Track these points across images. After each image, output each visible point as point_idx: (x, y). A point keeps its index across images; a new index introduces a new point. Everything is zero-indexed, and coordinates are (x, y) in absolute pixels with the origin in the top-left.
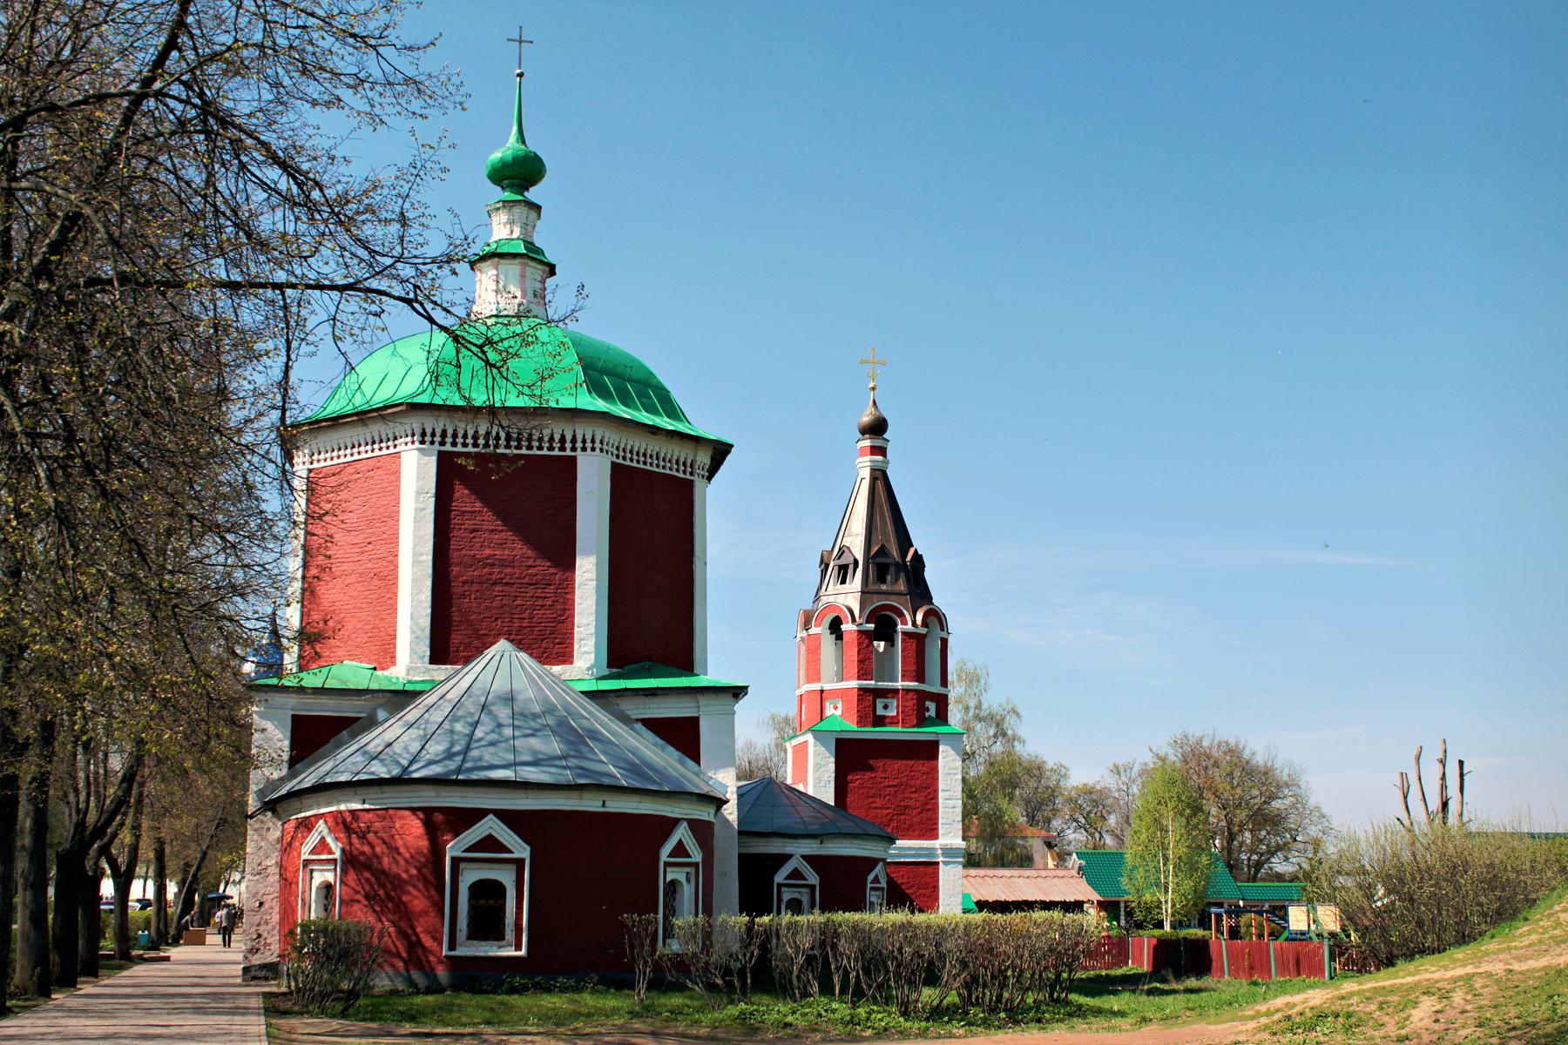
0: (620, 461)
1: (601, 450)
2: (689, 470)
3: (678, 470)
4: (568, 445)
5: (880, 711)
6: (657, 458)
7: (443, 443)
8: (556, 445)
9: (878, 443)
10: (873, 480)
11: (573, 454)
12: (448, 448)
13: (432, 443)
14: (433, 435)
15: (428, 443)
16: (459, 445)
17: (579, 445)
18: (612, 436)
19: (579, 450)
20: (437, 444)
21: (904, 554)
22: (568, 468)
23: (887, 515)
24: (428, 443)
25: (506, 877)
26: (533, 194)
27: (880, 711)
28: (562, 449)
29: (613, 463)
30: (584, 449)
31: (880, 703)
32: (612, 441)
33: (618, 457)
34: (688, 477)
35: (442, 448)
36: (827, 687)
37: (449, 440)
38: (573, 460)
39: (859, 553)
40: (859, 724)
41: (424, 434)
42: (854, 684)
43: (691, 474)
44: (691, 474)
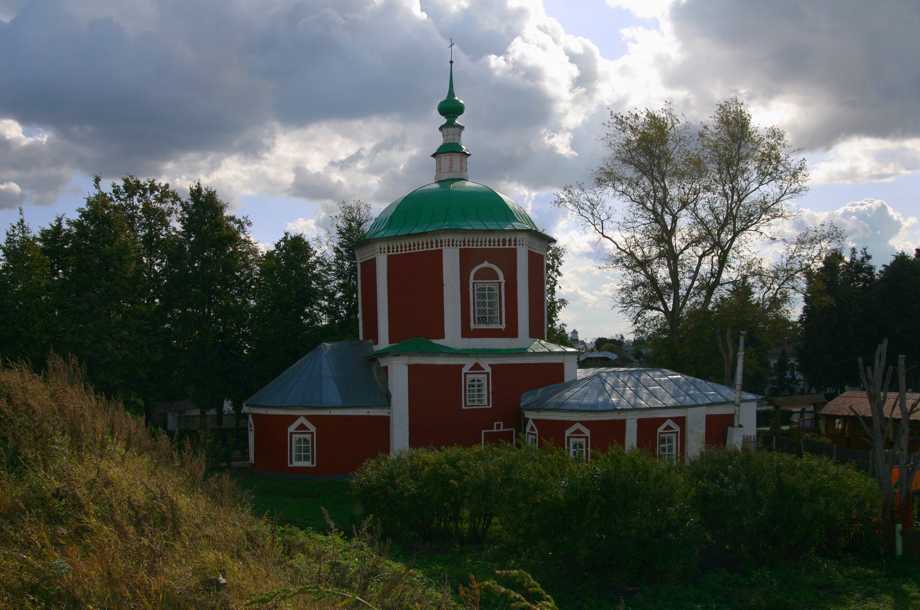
0: (467, 247)
2: (513, 243)
3: (503, 245)
4: (439, 244)
7: (389, 252)
8: (434, 245)
12: (391, 253)
14: (384, 249)
18: (458, 238)
22: (437, 256)
29: (461, 250)
30: (445, 246)
34: (513, 246)
37: (391, 250)
38: (442, 250)
41: (381, 249)
44: (515, 245)
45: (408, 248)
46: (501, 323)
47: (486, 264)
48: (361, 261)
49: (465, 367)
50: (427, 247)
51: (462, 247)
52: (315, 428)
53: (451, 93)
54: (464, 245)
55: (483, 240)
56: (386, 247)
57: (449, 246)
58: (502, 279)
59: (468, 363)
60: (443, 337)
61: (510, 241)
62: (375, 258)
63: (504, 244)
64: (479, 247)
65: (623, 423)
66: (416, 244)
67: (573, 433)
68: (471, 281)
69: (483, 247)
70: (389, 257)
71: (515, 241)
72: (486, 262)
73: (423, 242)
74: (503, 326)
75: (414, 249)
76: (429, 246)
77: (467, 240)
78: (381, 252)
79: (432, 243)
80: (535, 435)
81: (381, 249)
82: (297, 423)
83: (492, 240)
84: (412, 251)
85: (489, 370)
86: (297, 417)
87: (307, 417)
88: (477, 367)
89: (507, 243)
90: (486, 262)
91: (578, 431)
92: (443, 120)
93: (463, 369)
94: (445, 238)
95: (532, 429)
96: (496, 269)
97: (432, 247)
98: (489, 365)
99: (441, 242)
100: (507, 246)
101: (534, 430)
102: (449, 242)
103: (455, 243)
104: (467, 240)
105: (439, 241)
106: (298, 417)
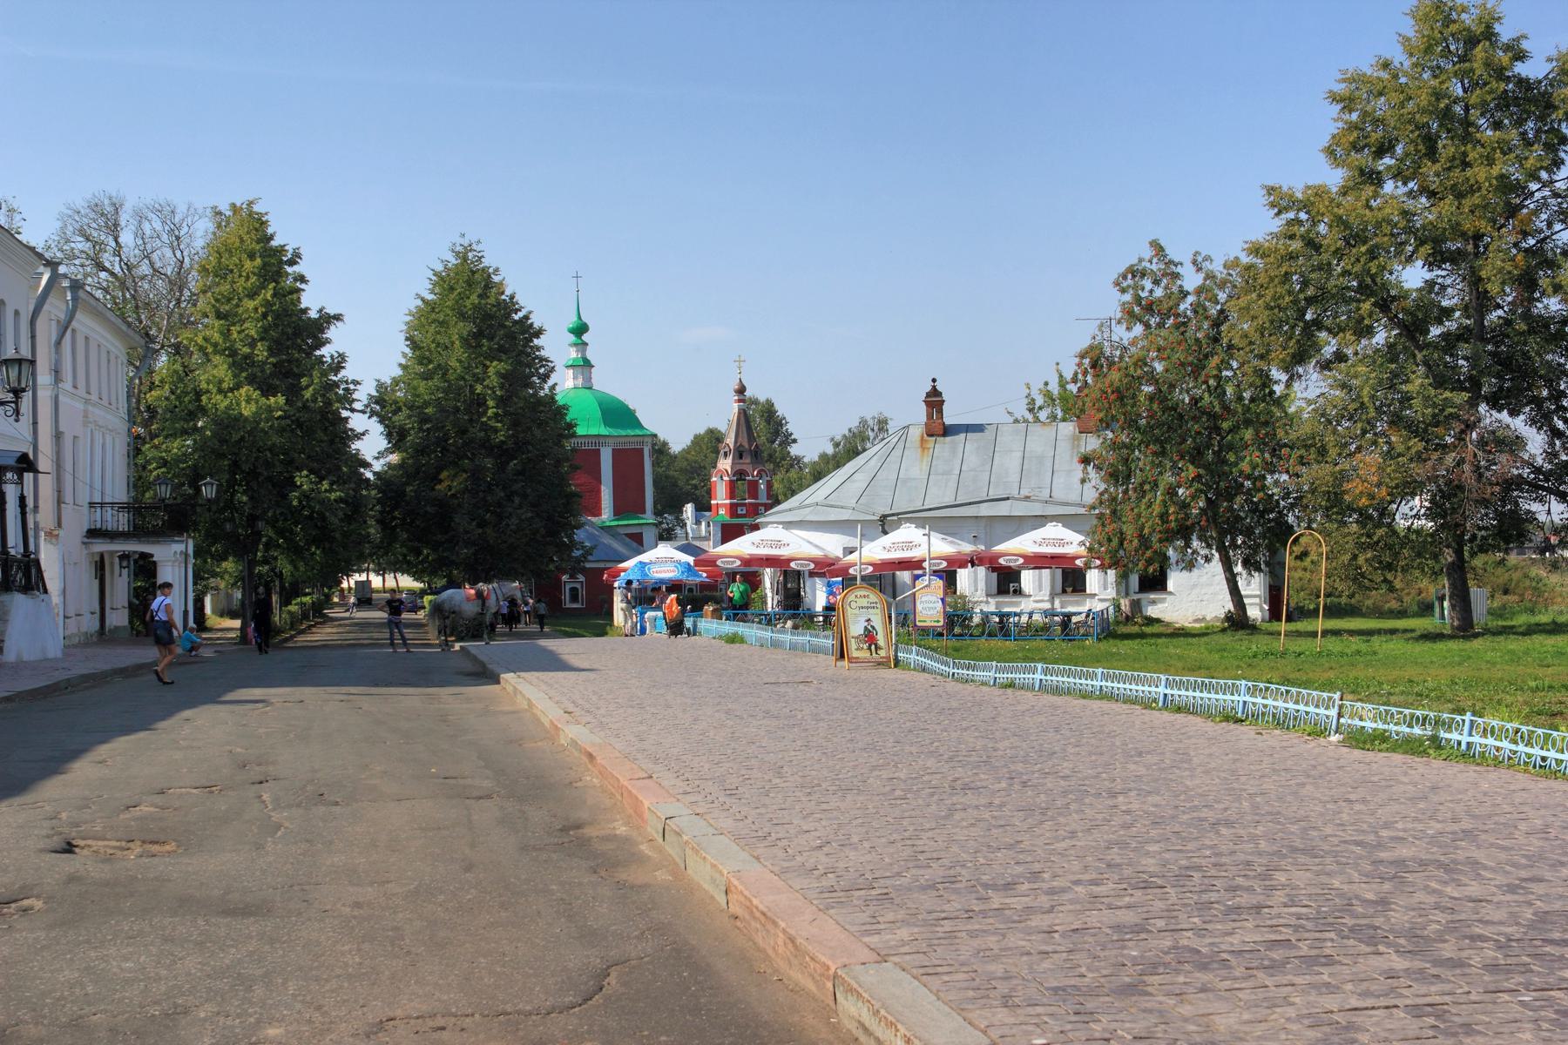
5: (739, 512)
9: (742, 397)
10: (739, 413)
18: (611, 441)
21: (750, 445)
22: (596, 454)
23: (745, 429)
25: (578, 586)
26: (585, 337)
27: (739, 512)
31: (739, 509)
36: (720, 502)
39: (732, 447)
40: (731, 517)
42: (728, 501)
53: (580, 318)
92: (572, 338)
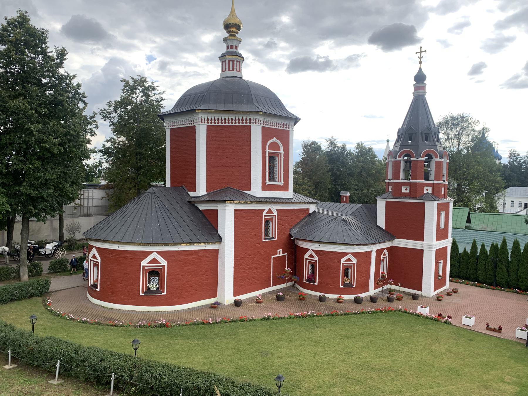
0: (265, 126)
1: (258, 123)
4: (248, 122)
6: (279, 124)
7: (208, 123)
8: (244, 122)
11: (250, 124)
12: (210, 124)
13: (204, 123)
14: (205, 120)
15: (203, 123)
16: (213, 123)
17: (252, 121)
18: (262, 119)
19: (252, 123)
20: (206, 123)
24: (203, 123)
28: (246, 123)
29: (262, 127)
30: (253, 123)
32: (262, 120)
33: (264, 124)
34: (287, 129)
35: (208, 124)
37: (210, 121)
41: (202, 120)
43: (289, 128)
45: (223, 122)
46: (281, 182)
47: (274, 140)
48: (172, 127)
49: (265, 211)
50: (239, 123)
51: (263, 126)
52: (166, 262)
54: (264, 124)
55: (274, 122)
56: (206, 119)
57: (256, 123)
58: (282, 151)
59: (266, 208)
60: (249, 189)
61: (286, 125)
62: (195, 126)
63: (283, 127)
64: (271, 127)
65: (369, 253)
66: (230, 119)
67: (345, 261)
68: (267, 151)
69: (273, 127)
70: (207, 126)
71: (289, 126)
72: (275, 138)
73: (235, 119)
74: (282, 183)
75: (229, 123)
76: (241, 122)
77: (265, 121)
78: (202, 122)
79: (242, 120)
80: (316, 261)
81: (202, 120)
82: (150, 258)
83: (278, 123)
84: (227, 124)
85: (275, 213)
86: (151, 252)
87: (158, 252)
88: (270, 211)
89: (285, 126)
90: (275, 138)
91: (349, 260)
93: (263, 213)
94: (253, 117)
95: (311, 256)
96: (279, 143)
97: (243, 123)
98: (276, 210)
99: (250, 119)
100: (285, 129)
101: (313, 257)
102: (256, 121)
103: (260, 122)
104: (265, 121)
105: (248, 119)
106: (151, 252)
